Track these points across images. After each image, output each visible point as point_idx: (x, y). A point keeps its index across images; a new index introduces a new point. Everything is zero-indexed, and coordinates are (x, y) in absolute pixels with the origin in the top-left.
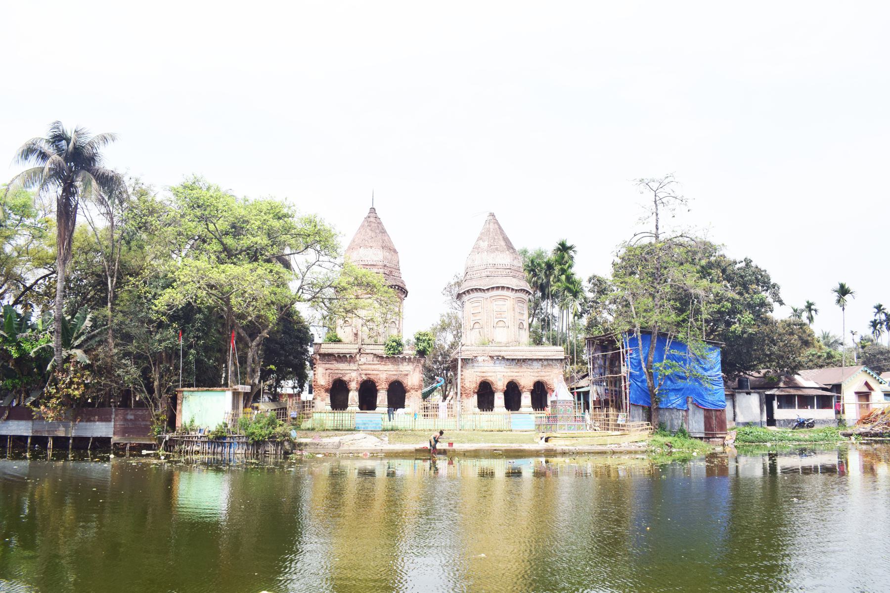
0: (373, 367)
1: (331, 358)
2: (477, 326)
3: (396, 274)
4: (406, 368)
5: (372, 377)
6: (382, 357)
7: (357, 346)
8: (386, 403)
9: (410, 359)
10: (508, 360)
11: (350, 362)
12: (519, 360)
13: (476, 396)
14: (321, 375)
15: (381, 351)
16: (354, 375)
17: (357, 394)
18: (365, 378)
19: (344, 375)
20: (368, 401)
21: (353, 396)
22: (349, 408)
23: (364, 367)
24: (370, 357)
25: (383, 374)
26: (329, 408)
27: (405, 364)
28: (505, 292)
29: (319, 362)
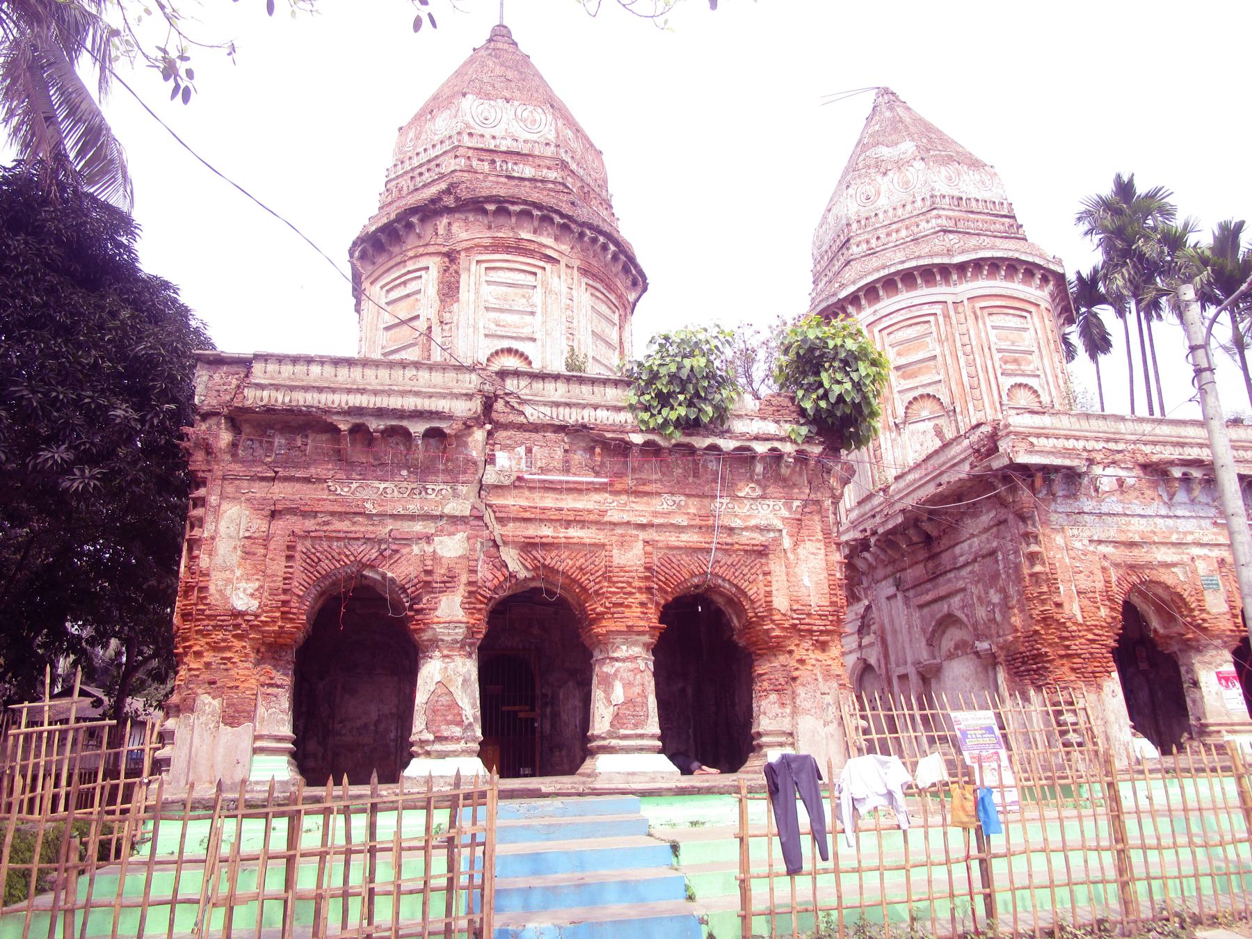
0: (571, 502)
1: (314, 442)
2: (926, 409)
3: (604, 213)
4: (756, 512)
5: (564, 562)
6: (621, 449)
7: (471, 382)
8: (653, 727)
9: (776, 457)
11: (423, 472)
14: (236, 555)
15: (611, 411)
16: (451, 547)
17: (467, 668)
18: (512, 559)
19: (392, 547)
20: (532, 728)
21: (448, 680)
22: (417, 768)
23: (512, 501)
24: (549, 452)
25: (630, 538)
26: (277, 770)
27: (745, 490)
28: (1017, 287)
29: (225, 465)
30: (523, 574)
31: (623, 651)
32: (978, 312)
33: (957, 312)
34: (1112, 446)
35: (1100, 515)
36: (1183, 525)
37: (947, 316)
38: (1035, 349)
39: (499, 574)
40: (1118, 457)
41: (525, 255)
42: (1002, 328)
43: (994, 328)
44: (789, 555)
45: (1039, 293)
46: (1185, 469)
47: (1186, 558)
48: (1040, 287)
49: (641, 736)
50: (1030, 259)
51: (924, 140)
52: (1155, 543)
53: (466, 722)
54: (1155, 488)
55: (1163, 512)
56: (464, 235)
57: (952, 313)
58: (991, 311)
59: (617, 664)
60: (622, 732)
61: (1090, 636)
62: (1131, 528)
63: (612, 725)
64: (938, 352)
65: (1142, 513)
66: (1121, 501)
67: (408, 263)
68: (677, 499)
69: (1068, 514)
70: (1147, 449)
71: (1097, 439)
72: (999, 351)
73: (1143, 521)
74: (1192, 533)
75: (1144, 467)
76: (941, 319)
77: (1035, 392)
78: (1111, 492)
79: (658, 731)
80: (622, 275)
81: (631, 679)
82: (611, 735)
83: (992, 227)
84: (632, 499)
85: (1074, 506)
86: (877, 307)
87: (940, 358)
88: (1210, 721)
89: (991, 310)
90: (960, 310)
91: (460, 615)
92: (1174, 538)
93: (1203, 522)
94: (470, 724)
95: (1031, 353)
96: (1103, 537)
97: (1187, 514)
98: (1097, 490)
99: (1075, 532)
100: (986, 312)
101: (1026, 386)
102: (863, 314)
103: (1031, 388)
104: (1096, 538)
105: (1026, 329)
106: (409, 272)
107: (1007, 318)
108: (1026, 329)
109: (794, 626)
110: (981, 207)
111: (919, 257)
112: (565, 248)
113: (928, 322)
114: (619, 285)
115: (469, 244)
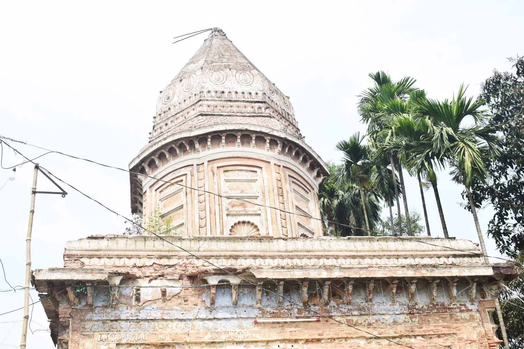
10: (269, 286)
12: (314, 286)
28: (252, 150)
32: (215, 170)
33: (198, 172)
34: (164, 262)
35: (138, 321)
36: (221, 326)
37: (192, 175)
38: (260, 195)
40: (170, 270)
42: (235, 181)
43: (227, 181)
45: (270, 153)
46: (221, 278)
50: (258, 129)
51: (217, 57)
52: (187, 343)
54: (200, 295)
55: (203, 315)
57: (195, 173)
58: (226, 169)
62: (169, 330)
64: (184, 203)
65: (181, 317)
66: (161, 308)
69: (104, 322)
70: (199, 263)
71: (149, 257)
72: (228, 198)
73: (182, 324)
74: (226, 332)
75: (192, 278)
76: (189, 177)
77: (256, 227)
78: (154, 301)
83: (244, 110)
85: (111, 314)
87: (185, 207)
89: (226, 168)
90: (201, 170)
92: (207, 339)
93: (245, 323)
95: (256, 198)
96: (132, 340)
97: (228, 316)
98: (138, 299)
99: (104, 337)
100: (222, 170)
101: (249, 222)
103: (253, 224)
104: (124, 341)
105: (255, 181)
107: (240, 173)
108: (255, 181)
110: (240, 97)
111: (173, 134)
113: (182, 181)
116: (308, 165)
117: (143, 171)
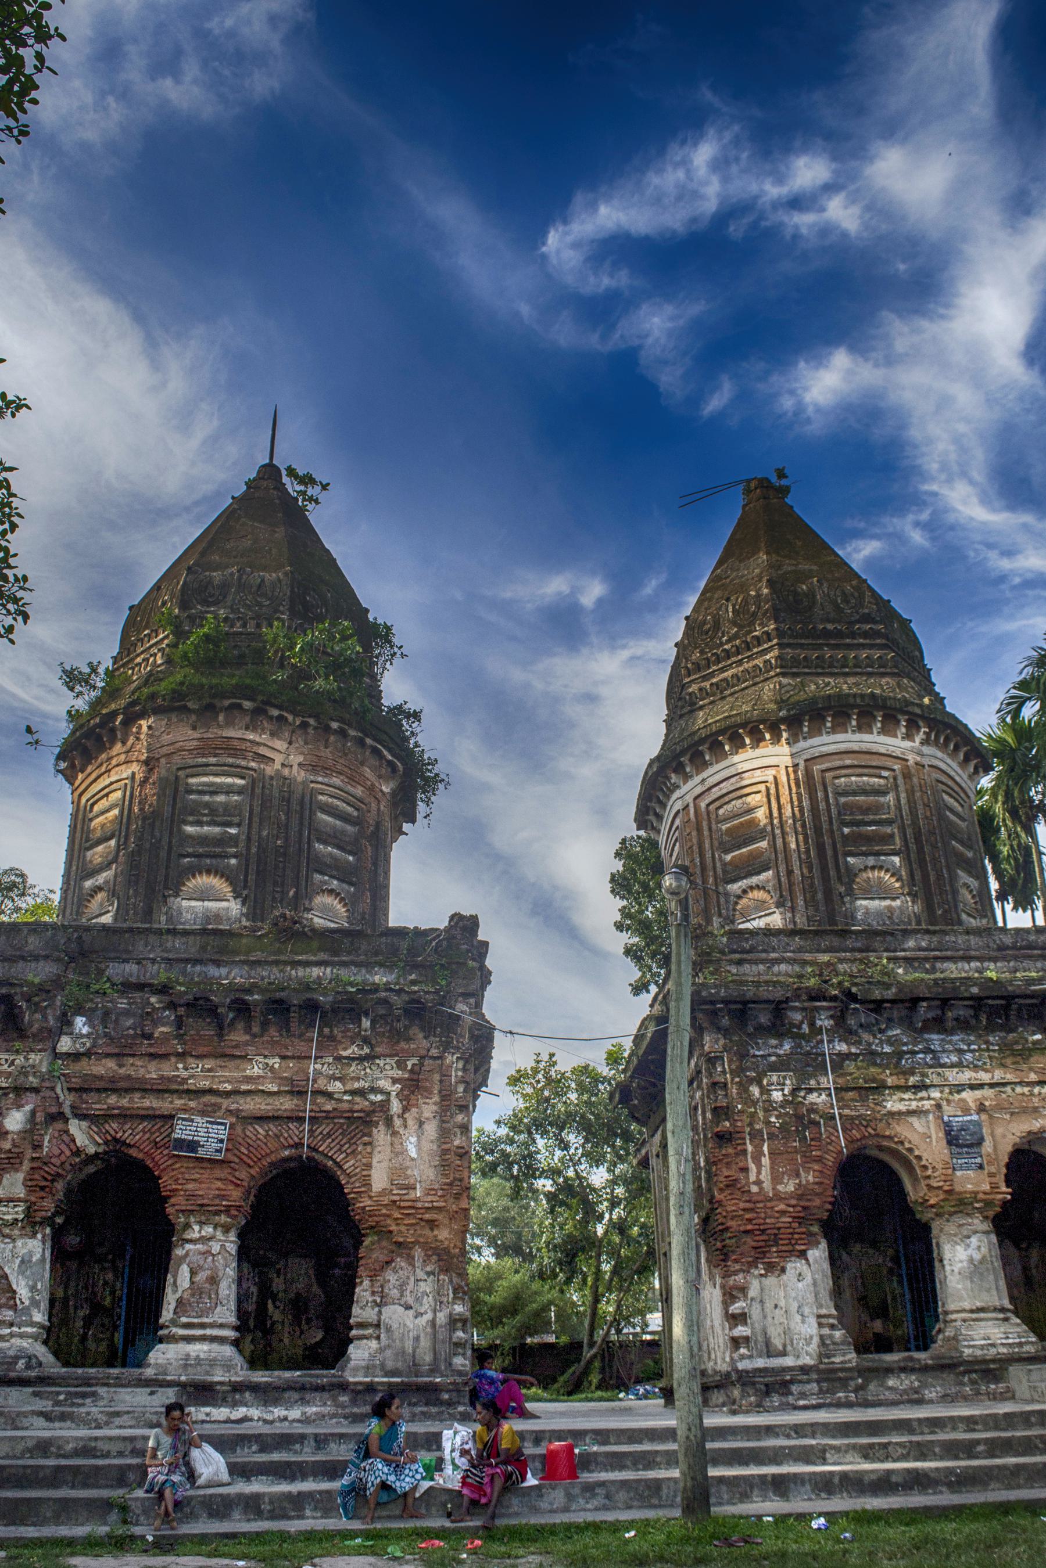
5: (134, 1134)
8: (226, 1314)
13: (818, 1253)
30: (91, 1150)
31: (196, 1232)
39: (63, 1147)
41: (234, 756)
44: (397, 1122)
45: (908, 744)
47: (927, 1104)
48: (908, 737)
49: (203, 1326)
53: (20, 1307)
56: (166, 738)
59: (188, 1246)
60: (184, 1320)
61: (782, 1207)
63: (175, 1313)
67: (113, 772)
68: (270, 1062)
79: (232, 1319)
80: (374, 762)
81: (201, 1262)
82: (174, 1322)
84: (218, 1062)
86: (705, 775)
88: (951, 1307)
91: (20, 1192)
94: (28, 1308)
102: (690, 784)
106: (112, 783)
109: (394, 1202)
112: (280, 744)
114: (367, 772)
115: (171, 749)
116: (961, 756)
117: (680, 769)
